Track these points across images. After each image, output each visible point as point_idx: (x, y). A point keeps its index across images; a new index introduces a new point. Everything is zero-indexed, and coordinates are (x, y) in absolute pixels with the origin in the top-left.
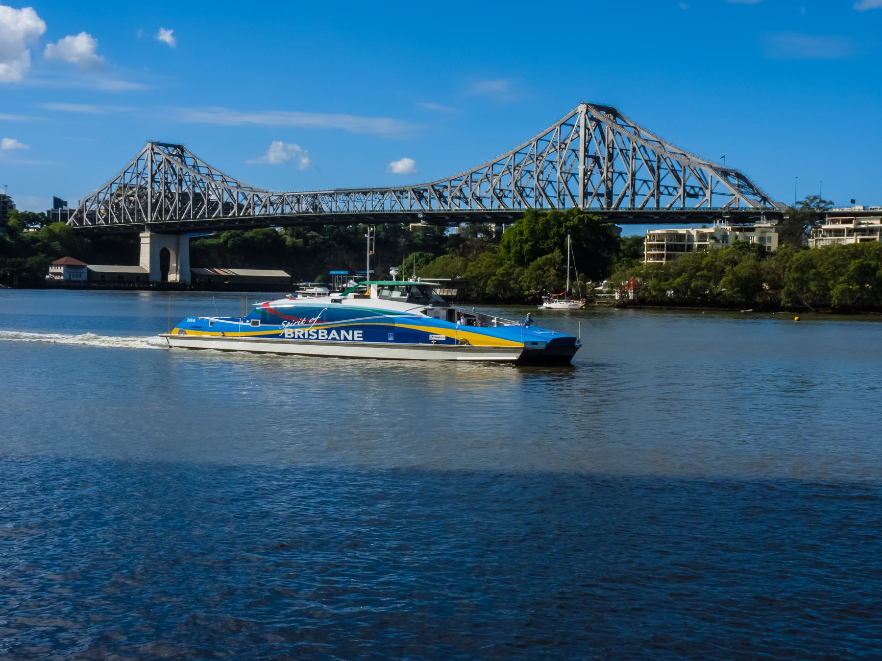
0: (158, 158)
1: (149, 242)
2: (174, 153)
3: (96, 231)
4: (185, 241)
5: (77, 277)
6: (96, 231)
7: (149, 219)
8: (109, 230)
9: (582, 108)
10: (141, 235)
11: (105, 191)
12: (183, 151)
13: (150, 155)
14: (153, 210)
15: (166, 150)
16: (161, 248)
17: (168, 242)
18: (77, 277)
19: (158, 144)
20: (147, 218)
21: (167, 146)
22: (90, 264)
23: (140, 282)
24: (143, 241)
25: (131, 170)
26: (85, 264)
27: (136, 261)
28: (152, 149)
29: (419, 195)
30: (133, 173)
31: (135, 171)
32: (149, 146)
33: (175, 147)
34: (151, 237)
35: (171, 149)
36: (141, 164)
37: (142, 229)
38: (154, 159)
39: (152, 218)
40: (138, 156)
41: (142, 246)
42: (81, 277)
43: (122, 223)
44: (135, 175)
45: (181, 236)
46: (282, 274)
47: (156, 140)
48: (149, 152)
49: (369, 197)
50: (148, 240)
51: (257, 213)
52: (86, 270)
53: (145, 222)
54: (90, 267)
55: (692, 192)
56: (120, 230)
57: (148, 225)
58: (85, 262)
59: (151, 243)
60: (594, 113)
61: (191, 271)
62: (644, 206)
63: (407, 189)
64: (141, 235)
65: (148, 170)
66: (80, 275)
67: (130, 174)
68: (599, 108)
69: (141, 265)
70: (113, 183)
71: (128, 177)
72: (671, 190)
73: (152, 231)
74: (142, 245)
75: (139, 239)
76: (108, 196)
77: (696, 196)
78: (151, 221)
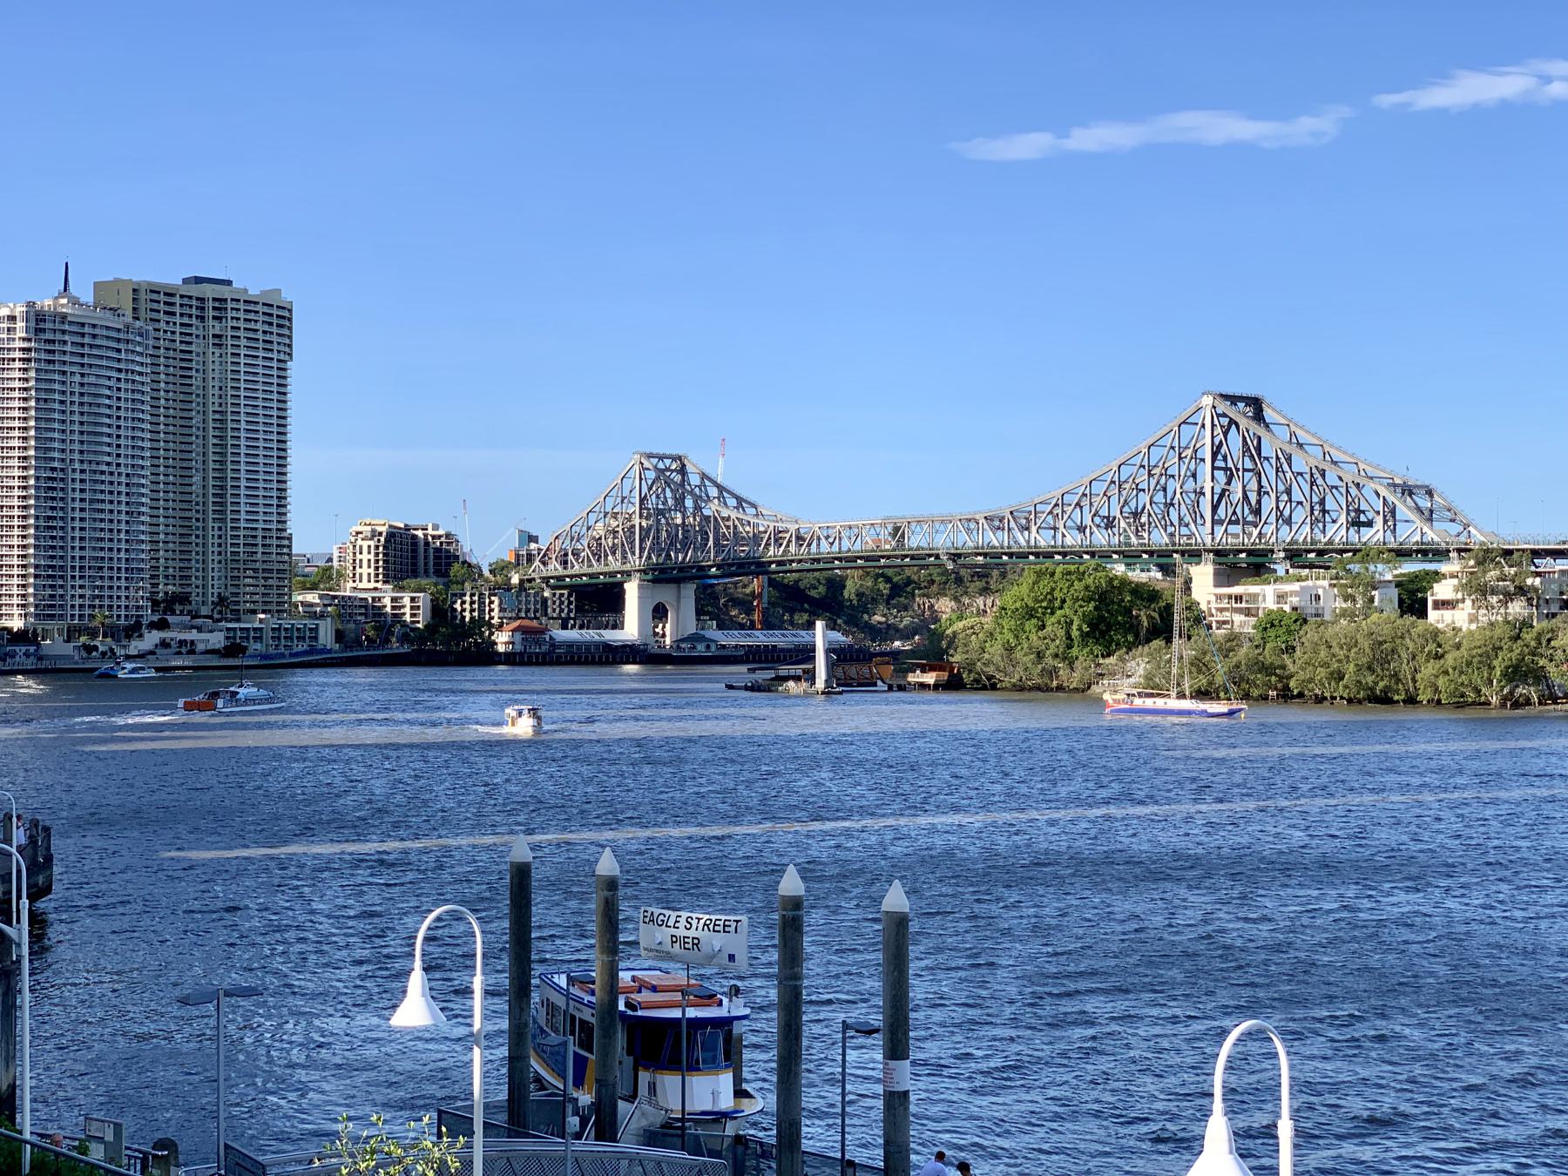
2: (673, 467)
4: (689, 591)
9: (1207, 401)
11: (580, 523)
12: (684, 466)
14: (642, 550)
17: (665, 594)
21: (661, 458)
23: (630, 653)
27: (619, 625)
29: (998, 523)
32: (637, 457)
33: (674, 458)
34: (640, 587)
35: (668, 462)
36: (627, 484)
44: (619, 500)
48: (637, 467)
55: (1363, 518)
60: (1223, 407)
63: (977, 517)
68: (1233, 399)
71: (610, 502)
72: (1334, 515)
76: (585, 529)
77: (1370, 524)
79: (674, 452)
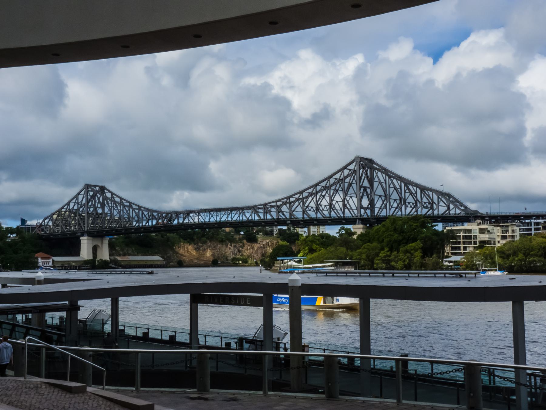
0: (91, 193)
3: (52, 237)
5: (46, 264)
6: (52, 237)
7: (86, 229)
8: (60, 236)
10: (81, 238)
13: (86, 192)
15: (95, 189)
16: (95, 244)
17: (97, 242)
18: (46, 264)
19: (91, 185)
20: (85, 228)
21: (95, 186)
22: (54, 256)
24: (82, 242)
25: (74, 201)
26: (50, 256)
27: (78, 254)
28: (88, 188)
30: (75, 202)
31: (77, 202)
34: (87, 239)
35: (97, 188)
36: (80, 197)
37: (82, 235)
38: (88, 194)
41: (82, 245)
42: (48, 264)
45: (104, 238)
46: (157, 258)
47: (90, 184)
49: (223, 213)
50: (86, 241)
52: (51, 260)
53: (83, 230)
56: (67, 235)
57: (86, 232)
58: (51, 255)
61: (110, 258)
64: (81, 238)
65: (84, 201)
67: (74, 203)
71: (72, 205)
73: (89, 236)
74: (82, 245)
75: (80, 241)
78: (87, 230)
79: (100, 185)
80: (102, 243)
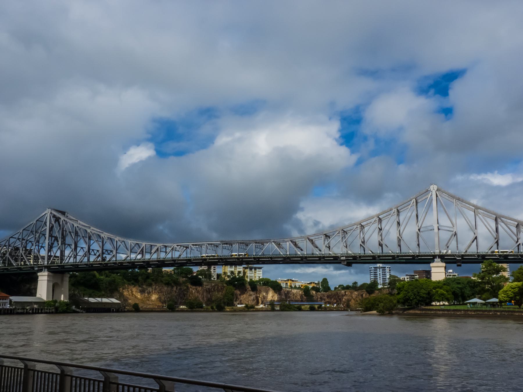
1: (46, 279)
4: (67, 279)
10: (39, 274)
13: (48, 218)
16: (54, 282)
24: (40, 278)
26: (8, 295)
27: (32, 292)
34: (48, 276)
37: (41, 271)
39: (48, 262)
40: (38, 218)
41: (39, 283)
43: (6, 266)
50: (46, 278)
51: (78, 261)
52: (9, 300)
54: (11, 298)
58: (9, 295)
59: (48, 280)
62: (466, 251)
64: (39, 274)
66: (5, 304)
69: (38, 295)
70: (11, 237)
73: (48, 271)
74: (39, 281)
75: (37, 277)
78: (48, 264)
80: (62, 281)
